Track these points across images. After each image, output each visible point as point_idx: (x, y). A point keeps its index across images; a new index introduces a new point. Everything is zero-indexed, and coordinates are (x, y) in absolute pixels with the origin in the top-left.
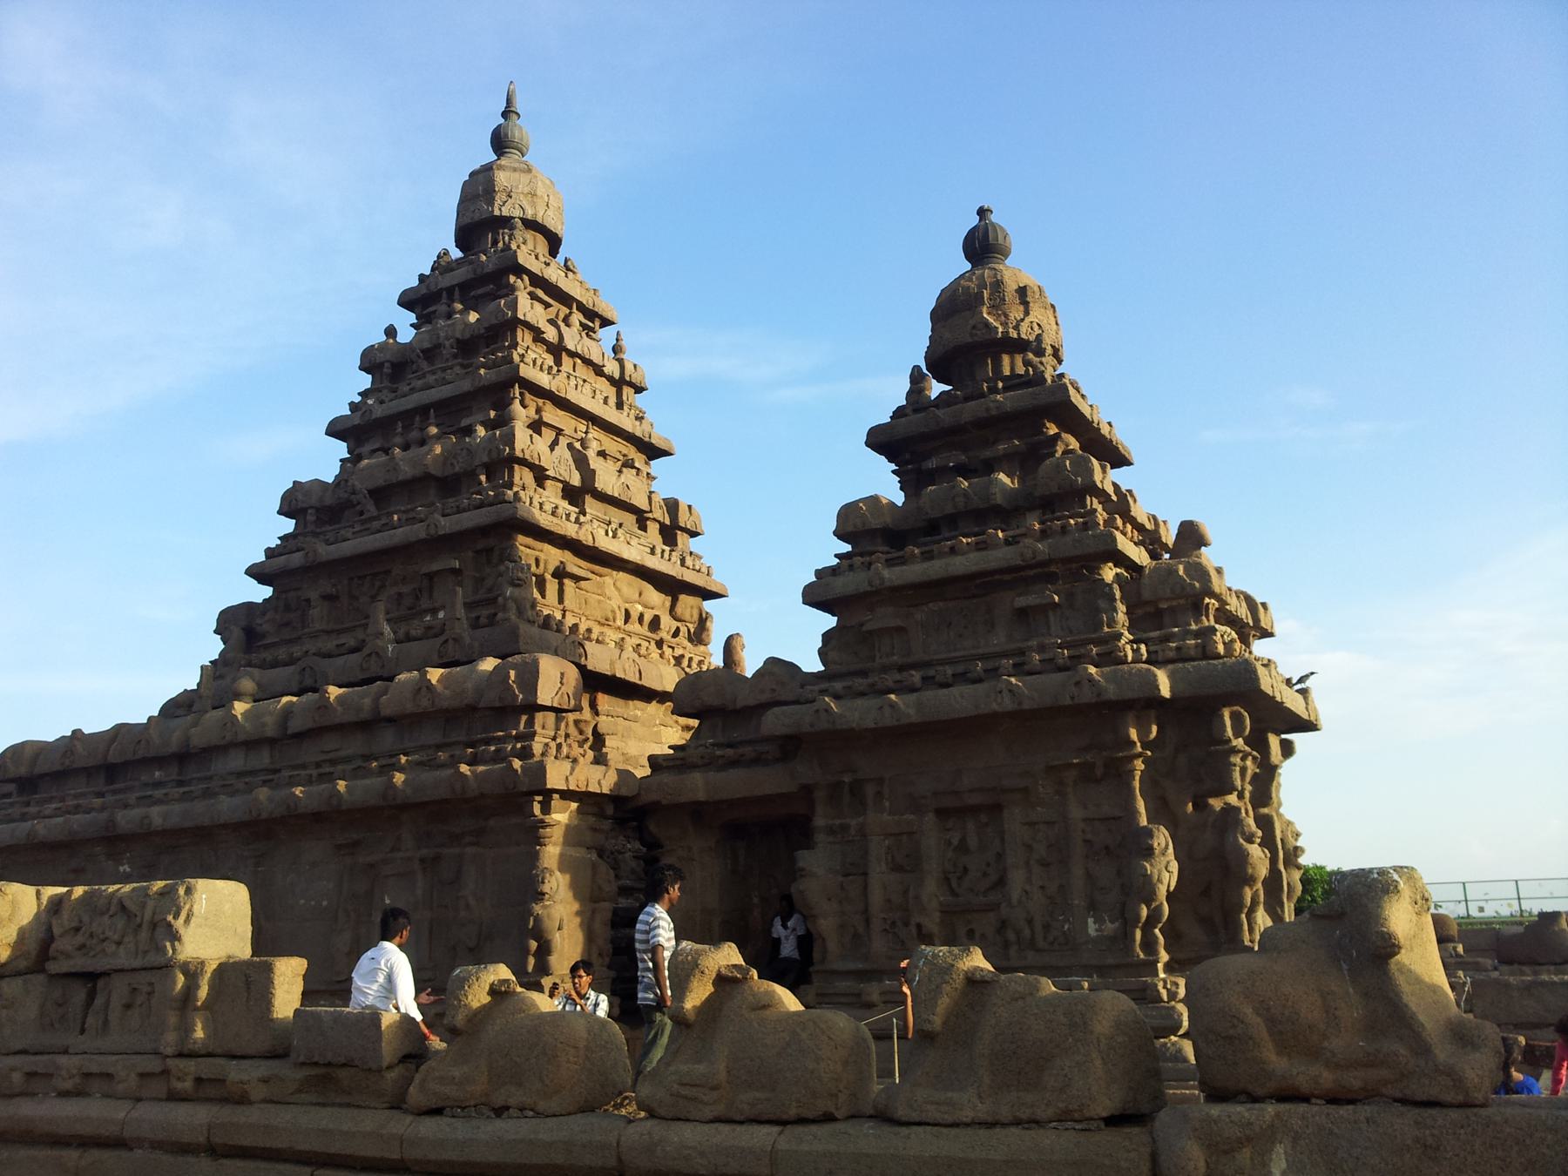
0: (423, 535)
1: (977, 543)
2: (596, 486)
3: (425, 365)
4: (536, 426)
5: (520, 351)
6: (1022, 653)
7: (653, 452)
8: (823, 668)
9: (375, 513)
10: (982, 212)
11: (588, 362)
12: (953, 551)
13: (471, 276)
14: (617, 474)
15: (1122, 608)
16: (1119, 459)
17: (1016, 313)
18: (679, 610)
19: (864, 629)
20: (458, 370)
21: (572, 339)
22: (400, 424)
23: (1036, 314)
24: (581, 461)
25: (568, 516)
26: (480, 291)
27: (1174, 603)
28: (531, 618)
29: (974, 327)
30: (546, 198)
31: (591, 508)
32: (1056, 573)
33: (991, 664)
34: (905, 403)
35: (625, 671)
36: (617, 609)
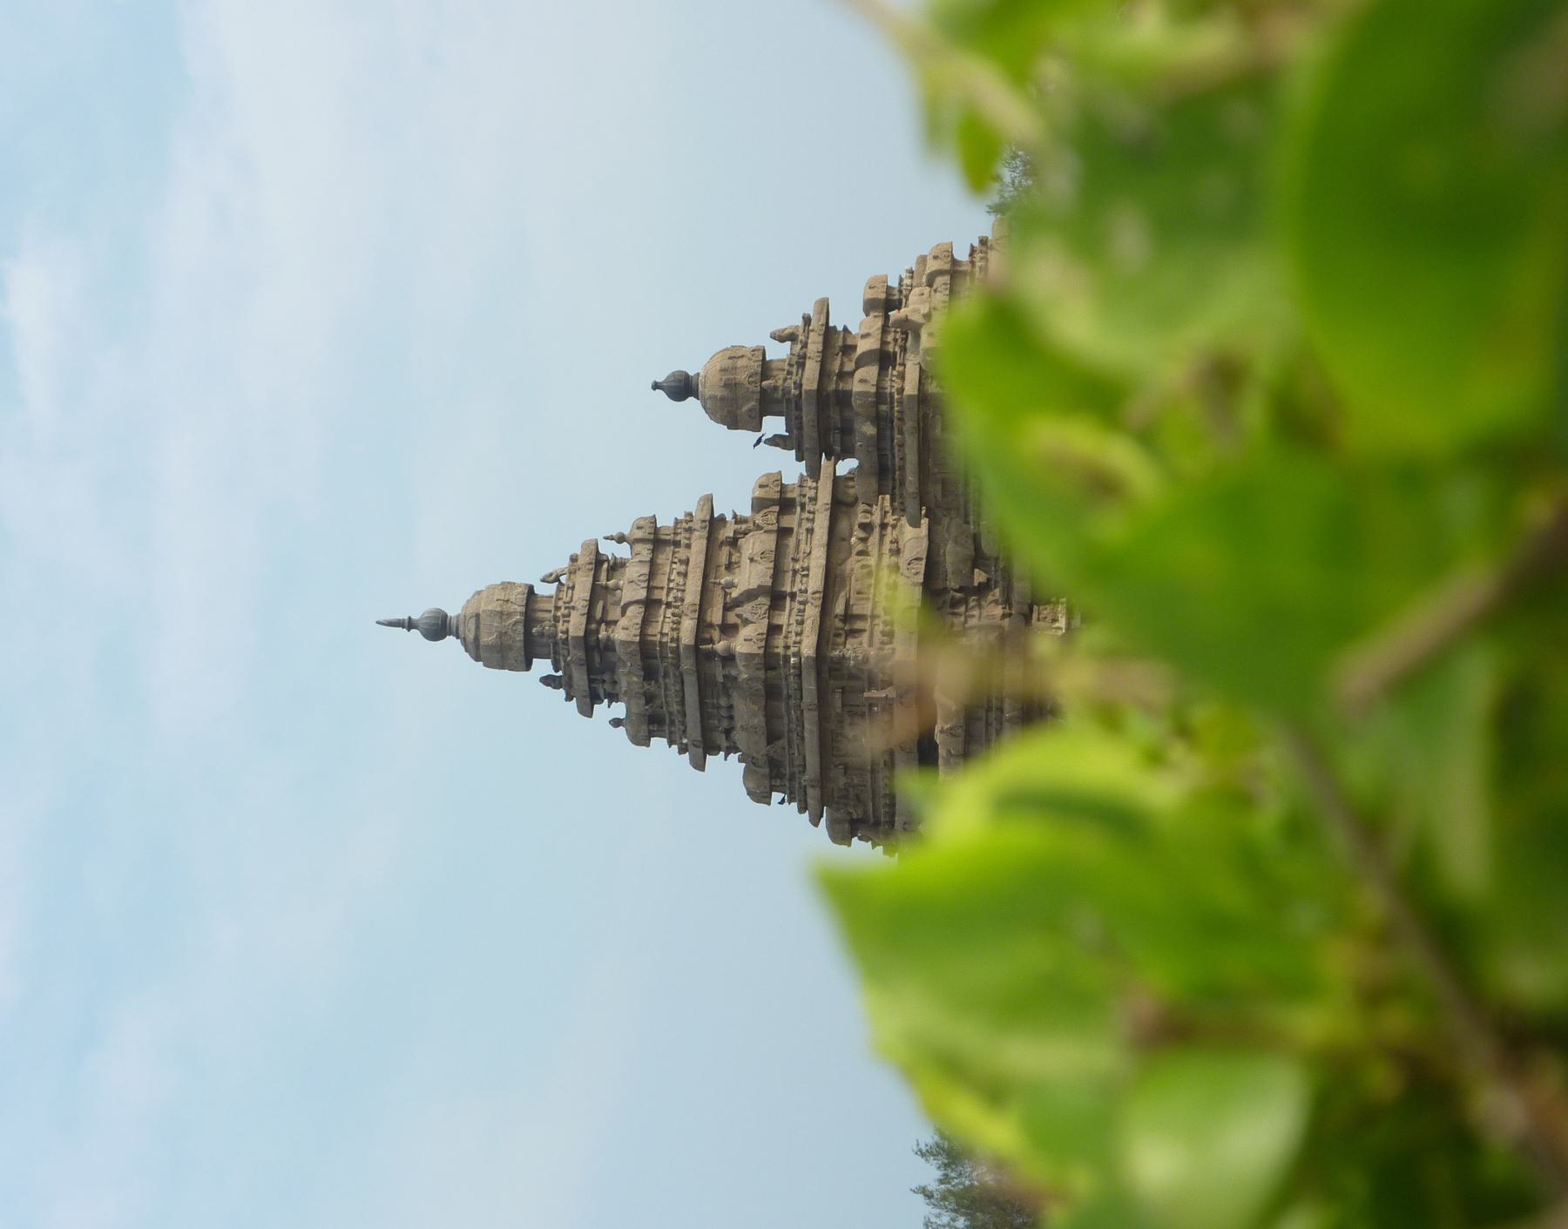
0: (816, 713)
2: (770, 584)
3: (658, 702)
4: (728, 629)
5: (664, 640)
9: (786, 740)
10: (656, 386)
12: (902, 459)
13: (585, 668)
14: (753, 564)
16: (824, 307)
19: (940, 499)
20: (671, 680)
21: (631, 588)
22: (711, 721)
23: (742, 377)
24: (750, 595)
25: (799, 611)
26: (597, 659)
29: (750, 416)
31: (783, 585)
35: (917, 573)
36: (860, 564)
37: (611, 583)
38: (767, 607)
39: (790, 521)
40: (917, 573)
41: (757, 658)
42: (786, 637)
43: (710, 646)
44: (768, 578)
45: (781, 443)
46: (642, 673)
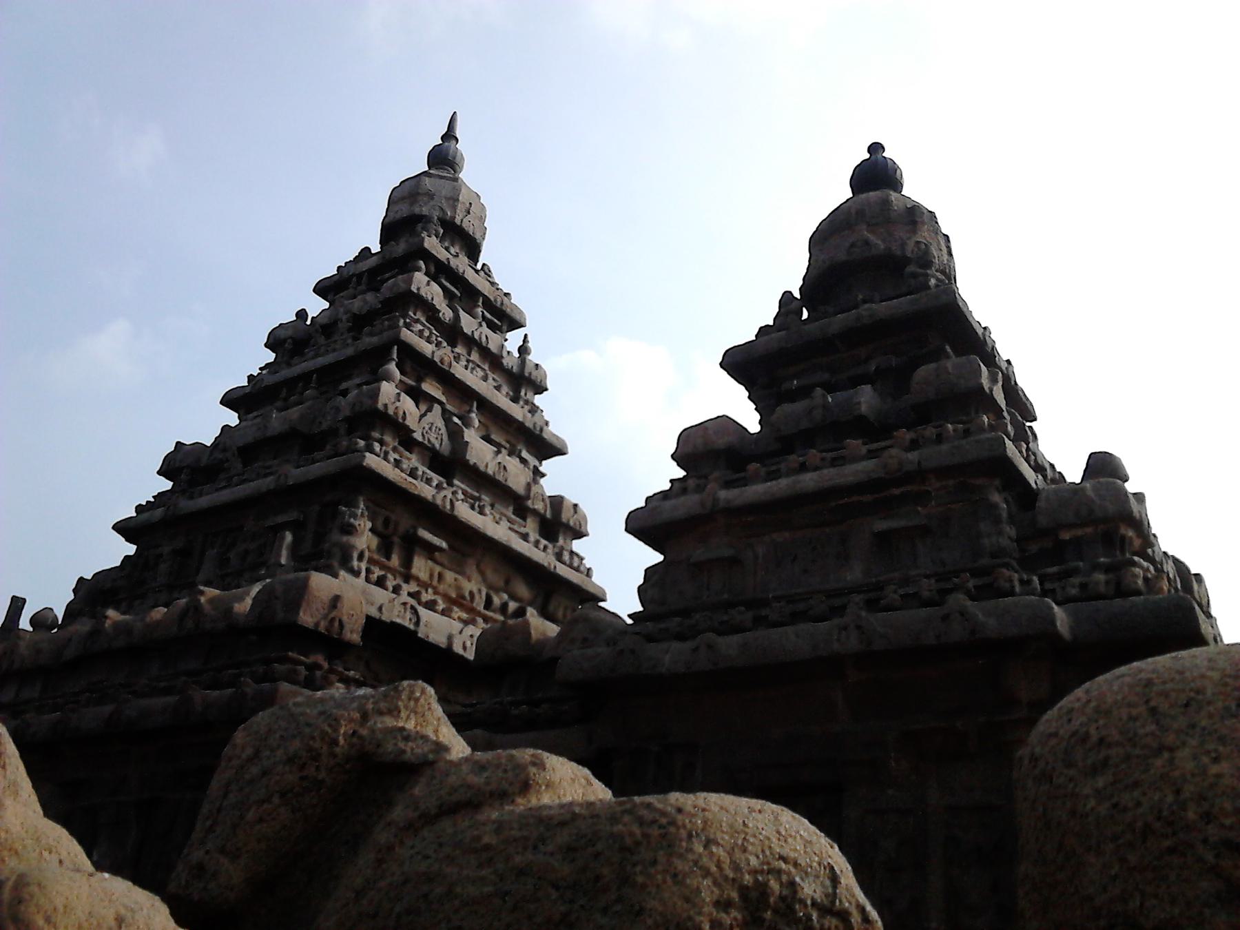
1: (834, 459)
3: (322, 340)
6: (879, 587)
7: (548, 449)
8: (641, 609)
10: (875, 148)
11: (485, 353)
12: (803, 468)
15: (1011, 531)
17: (900, 233)
18: (551, 608)
20: (350, 341)
23: (924, 235)
24: (455, 435)
27: (1079, 532)
28: (356, 568)
29: (853, 245)
30: (468, 205)
32: (928, 492)
33: (837, 602)
34: (771, 323)
35: (465, 648)
37: (479, 310)
38: (437, 446)
39: (531, 527)
40: (465, 648)
41: (370, 402)
42: (395, 449)
43: (395, 356)
44: (475, 461)
45: (794, 305)
46: (364, 311)
